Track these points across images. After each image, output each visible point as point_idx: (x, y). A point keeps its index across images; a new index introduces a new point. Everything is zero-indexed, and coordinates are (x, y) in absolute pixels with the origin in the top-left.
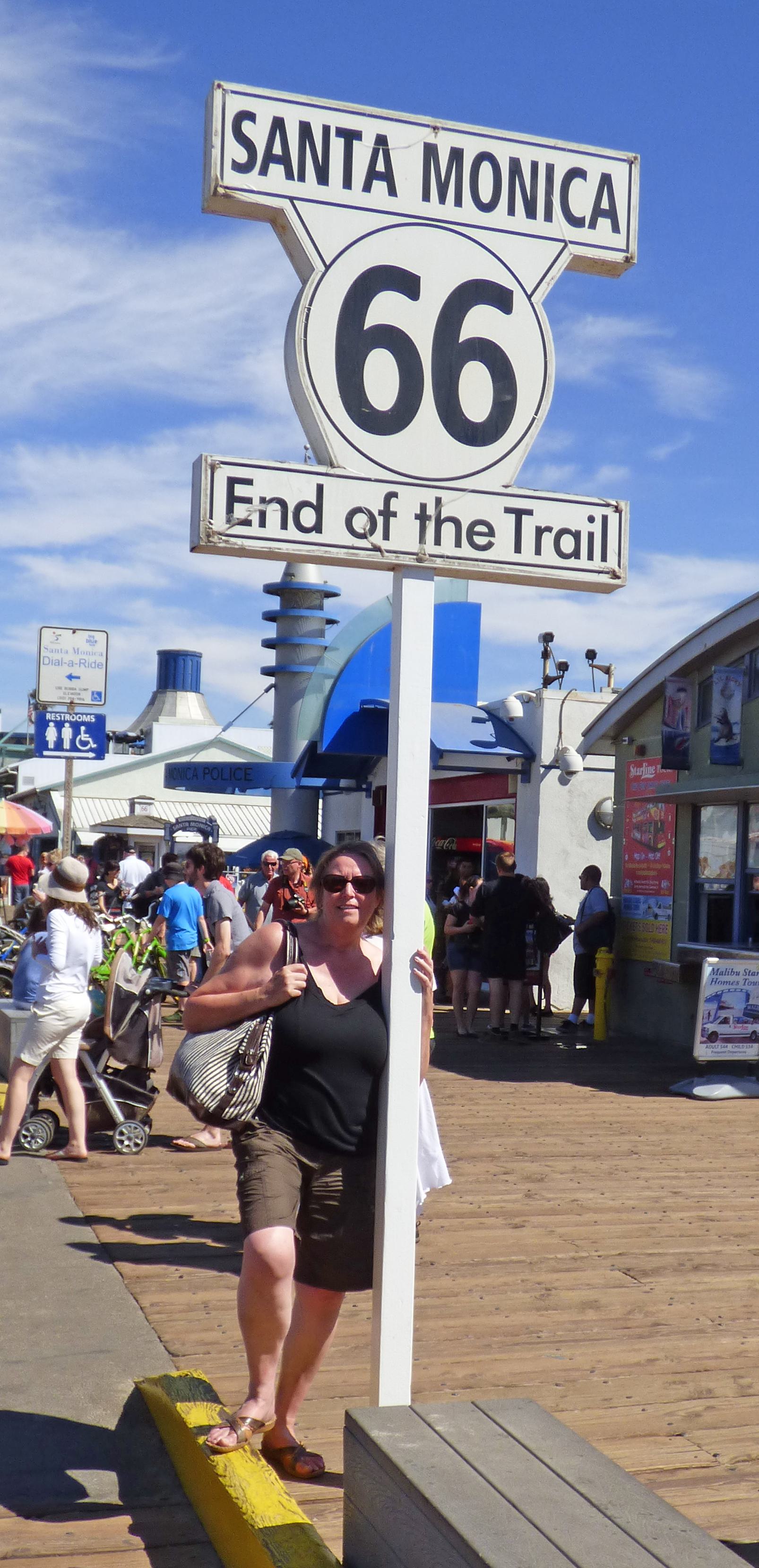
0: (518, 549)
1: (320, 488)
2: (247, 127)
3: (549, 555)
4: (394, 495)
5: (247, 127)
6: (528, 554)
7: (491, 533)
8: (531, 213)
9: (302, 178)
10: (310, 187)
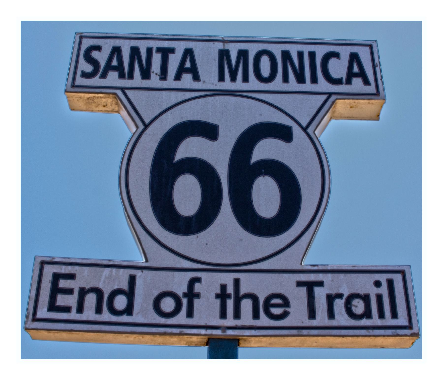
0: (312, 314)
1: (132, 280)
2: (95, 54)
3: (341, 318)
4: (198, 280)
5: (95, 54)
6: (322, 318)
7: (286, 303)
8: (301, 79)
9: (131, 76)
10: (137, 80)
